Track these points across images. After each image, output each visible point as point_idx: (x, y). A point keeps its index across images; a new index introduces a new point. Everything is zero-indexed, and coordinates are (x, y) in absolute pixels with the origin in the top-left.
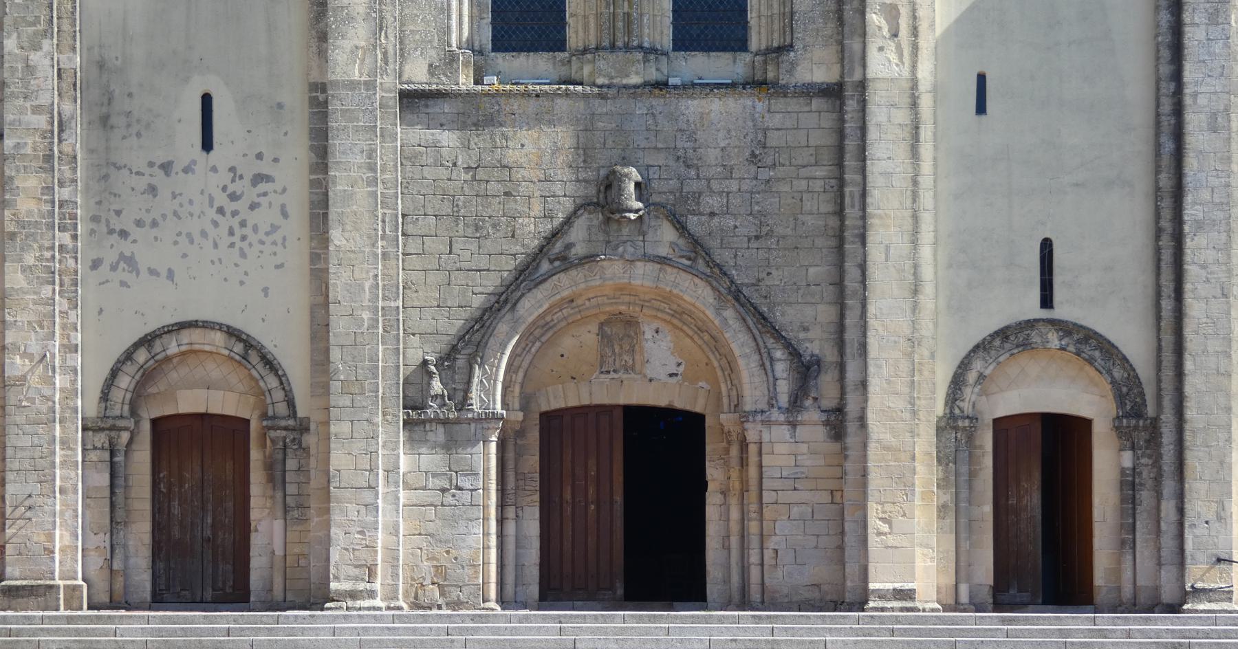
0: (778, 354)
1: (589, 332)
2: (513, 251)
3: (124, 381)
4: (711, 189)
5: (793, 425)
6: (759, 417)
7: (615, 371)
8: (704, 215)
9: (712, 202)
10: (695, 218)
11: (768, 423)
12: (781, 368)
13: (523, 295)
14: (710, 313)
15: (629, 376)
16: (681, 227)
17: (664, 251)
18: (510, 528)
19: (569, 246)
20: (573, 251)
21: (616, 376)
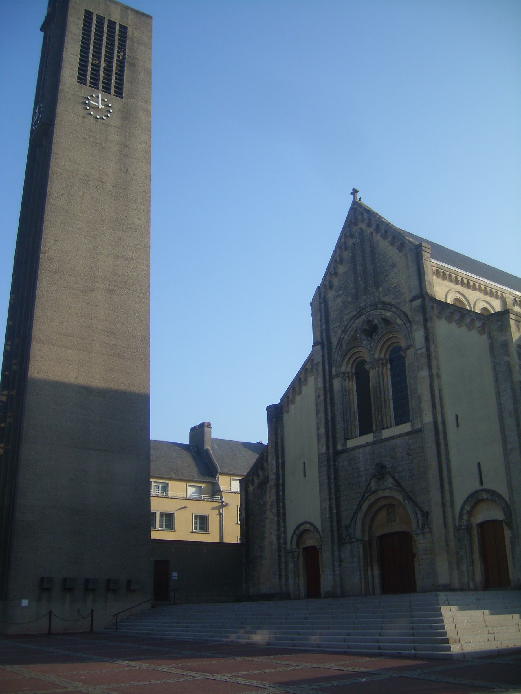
0: (418, 512)
3: (295, 539)
5: (424, 533)
6: (415, 533)
9: (400, 468)
11: (417, 534)
12: (419, 516)
14: (402, 501)
16: (393, 477)
17: (390, 485)
18: (370, 573)
19: (371, 488)
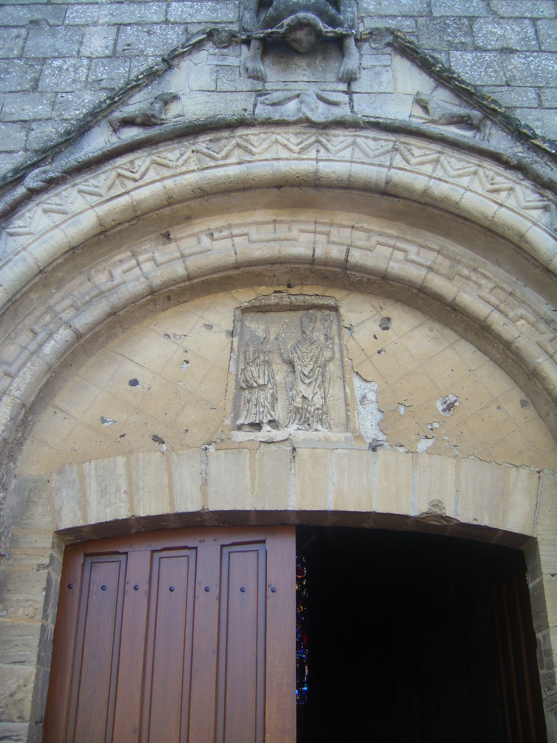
1: (209, 327)
2: (29, 112)
4: (495, 13)
7: (273, 423)
8: (487, 51)
10: (469, 56)
13: (33, 193)
15: (311, 434)
20: (174, 109)
21: (278, 435)
